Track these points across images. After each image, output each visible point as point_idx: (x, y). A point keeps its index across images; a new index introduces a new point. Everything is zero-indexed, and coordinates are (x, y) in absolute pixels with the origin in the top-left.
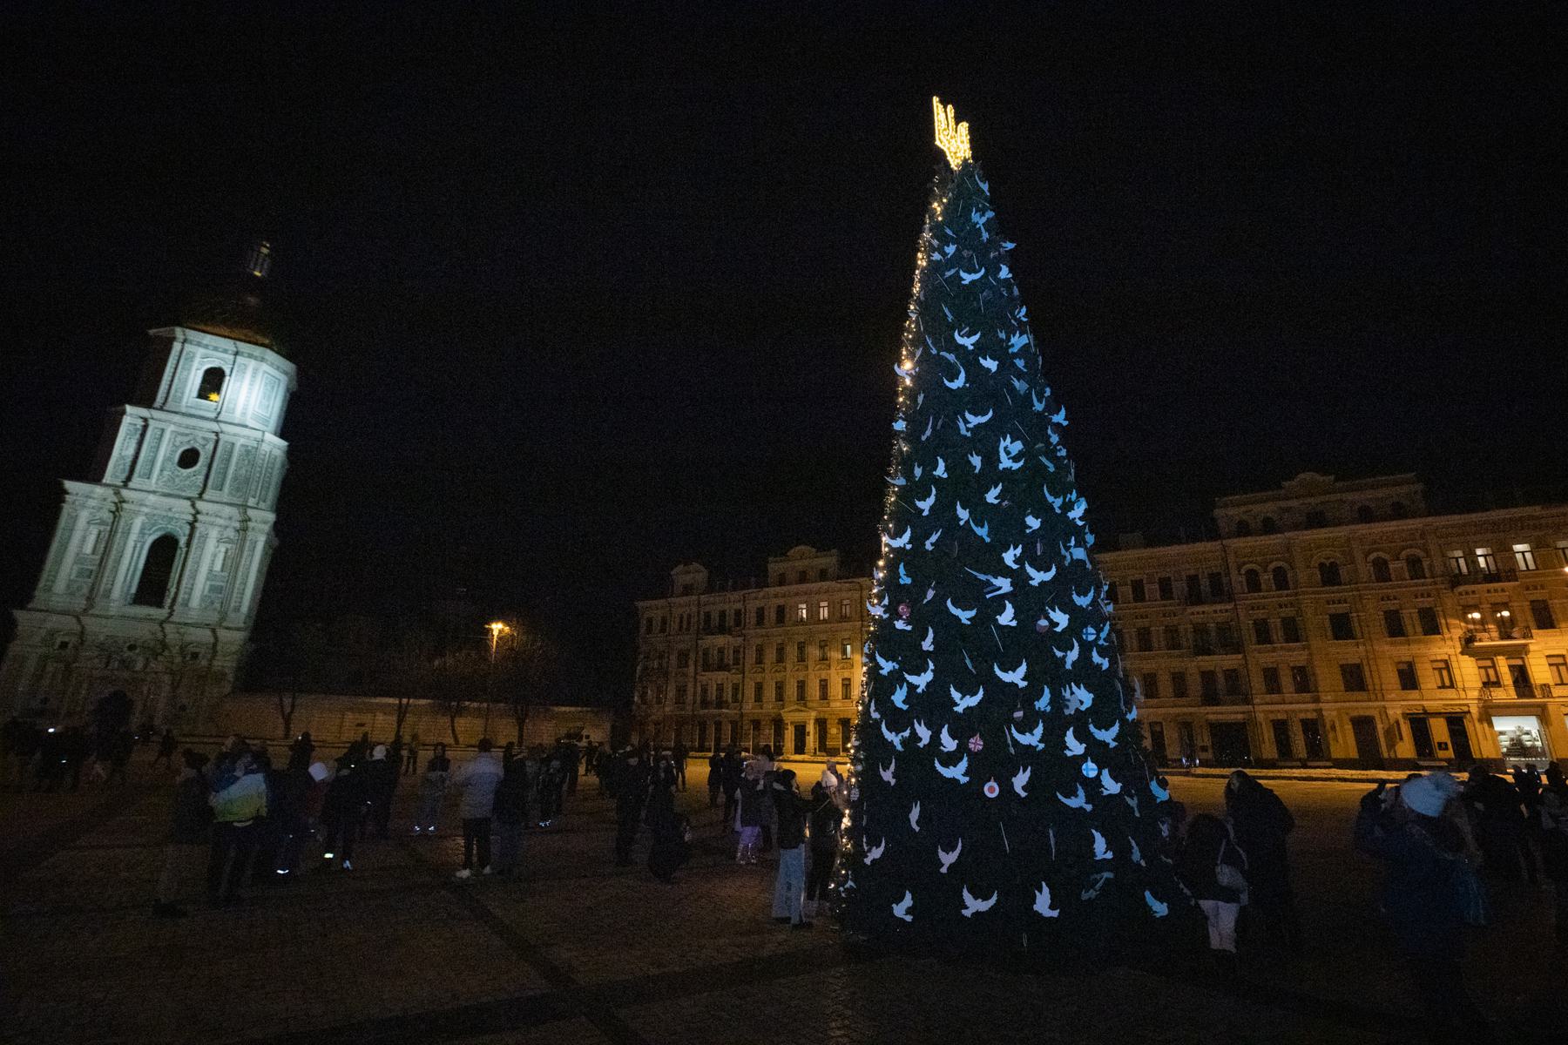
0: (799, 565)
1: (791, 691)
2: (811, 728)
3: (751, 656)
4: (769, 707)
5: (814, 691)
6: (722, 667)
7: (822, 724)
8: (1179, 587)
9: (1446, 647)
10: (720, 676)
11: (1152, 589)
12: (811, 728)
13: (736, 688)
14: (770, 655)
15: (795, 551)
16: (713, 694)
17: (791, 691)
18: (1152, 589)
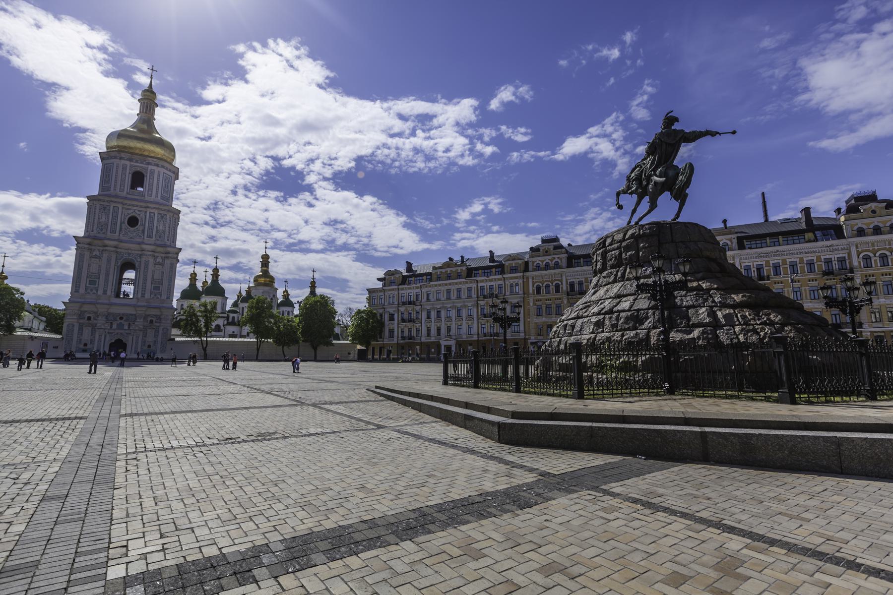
10: (410, 324)
13: (418, 331)
14: (433, 314)
16: (406, 334)
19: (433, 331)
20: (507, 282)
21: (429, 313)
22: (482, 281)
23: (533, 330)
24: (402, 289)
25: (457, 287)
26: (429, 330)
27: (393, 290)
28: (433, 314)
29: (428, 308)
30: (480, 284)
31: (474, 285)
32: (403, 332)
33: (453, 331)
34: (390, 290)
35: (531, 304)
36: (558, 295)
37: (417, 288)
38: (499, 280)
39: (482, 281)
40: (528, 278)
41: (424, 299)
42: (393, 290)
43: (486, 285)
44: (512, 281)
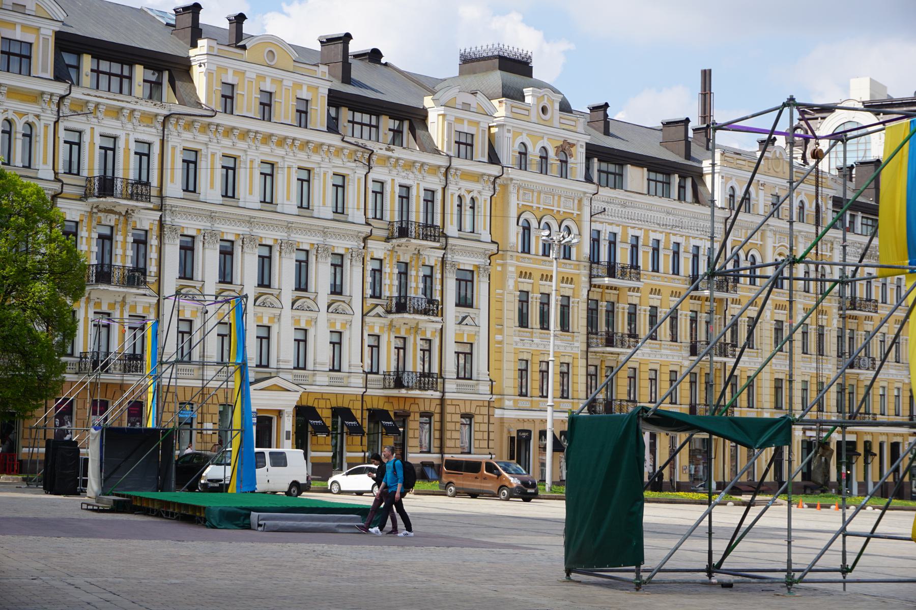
2: (288, 424)
14: (208, 261)
20: (452, 189)
21: (187, 249)
23: (509, 381)
25: (303, 158)
28: (208, 261)
29: (191, 226)
30: (378, 173)
31: (355, 173)
33: (284, 350)
35: (511, 283)
36: (569, 269)
38: (435, 169)
40: (505, 186)
41: (174, 188)
43: (393, 179)
44: (466, 185)
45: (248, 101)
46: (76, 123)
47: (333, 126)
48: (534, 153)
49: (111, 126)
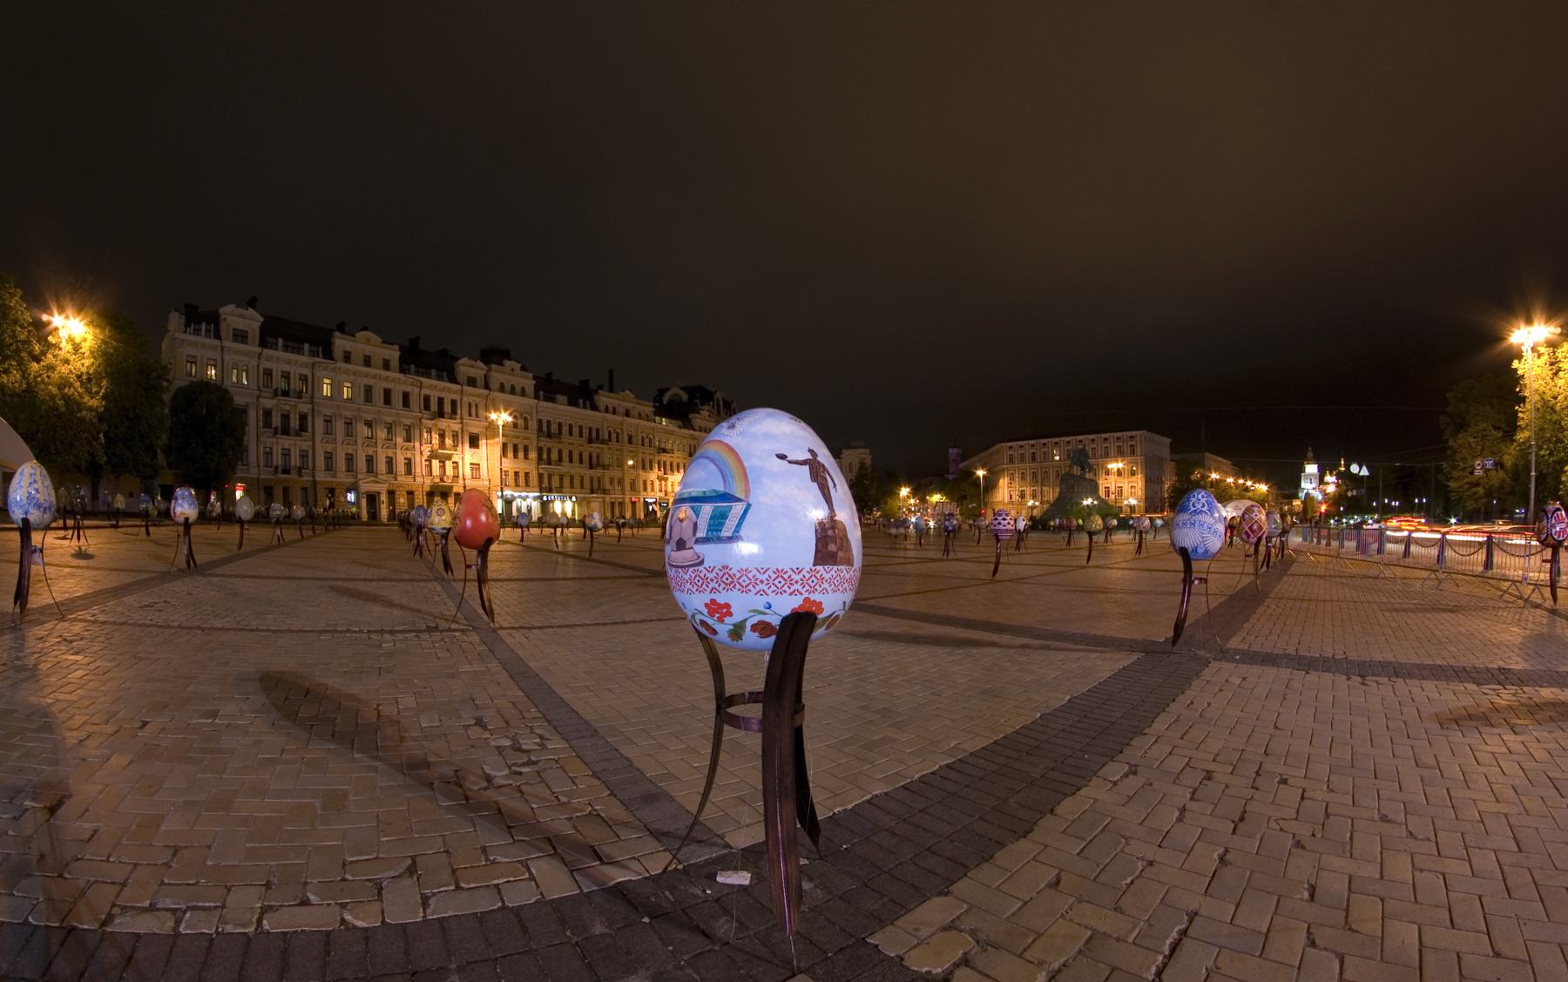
0: (368, 350)
1: (361, 464)
2: (384, 497)
3: (320, 425)
4: (343, 477)
5: (382, 466)
6: (286, 431)
7: (391, 493)
8: (586, 432)
9: (653, 476)
11: (576, 430)
12: (384, 497)
13: (304, 455)
14: (340, 427)
15: (361, 335)
16: (278, 460)
17: (361, 464)
18: (576, 430)
19: (341, 464)
22: (430, 387)
24: (269, 359)
26: (329, 457)
27: (248, 354)
28: (340, 427)
30: (425, 391)
32: (269, 454)
34: (236, 352)
37: (305, 365)
39: (430, 387)
42: (248, 354)
43: (434, 396)
45: (357, 356)
46: (269, 365)
47: (402, 371)
48: (508, 387)
49: (286, 367)
